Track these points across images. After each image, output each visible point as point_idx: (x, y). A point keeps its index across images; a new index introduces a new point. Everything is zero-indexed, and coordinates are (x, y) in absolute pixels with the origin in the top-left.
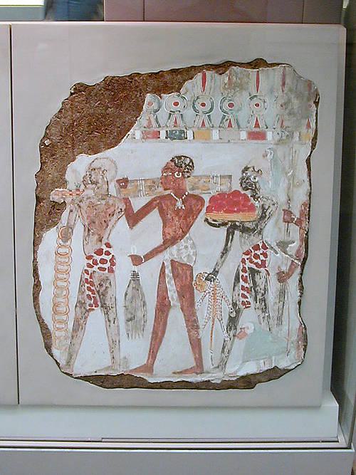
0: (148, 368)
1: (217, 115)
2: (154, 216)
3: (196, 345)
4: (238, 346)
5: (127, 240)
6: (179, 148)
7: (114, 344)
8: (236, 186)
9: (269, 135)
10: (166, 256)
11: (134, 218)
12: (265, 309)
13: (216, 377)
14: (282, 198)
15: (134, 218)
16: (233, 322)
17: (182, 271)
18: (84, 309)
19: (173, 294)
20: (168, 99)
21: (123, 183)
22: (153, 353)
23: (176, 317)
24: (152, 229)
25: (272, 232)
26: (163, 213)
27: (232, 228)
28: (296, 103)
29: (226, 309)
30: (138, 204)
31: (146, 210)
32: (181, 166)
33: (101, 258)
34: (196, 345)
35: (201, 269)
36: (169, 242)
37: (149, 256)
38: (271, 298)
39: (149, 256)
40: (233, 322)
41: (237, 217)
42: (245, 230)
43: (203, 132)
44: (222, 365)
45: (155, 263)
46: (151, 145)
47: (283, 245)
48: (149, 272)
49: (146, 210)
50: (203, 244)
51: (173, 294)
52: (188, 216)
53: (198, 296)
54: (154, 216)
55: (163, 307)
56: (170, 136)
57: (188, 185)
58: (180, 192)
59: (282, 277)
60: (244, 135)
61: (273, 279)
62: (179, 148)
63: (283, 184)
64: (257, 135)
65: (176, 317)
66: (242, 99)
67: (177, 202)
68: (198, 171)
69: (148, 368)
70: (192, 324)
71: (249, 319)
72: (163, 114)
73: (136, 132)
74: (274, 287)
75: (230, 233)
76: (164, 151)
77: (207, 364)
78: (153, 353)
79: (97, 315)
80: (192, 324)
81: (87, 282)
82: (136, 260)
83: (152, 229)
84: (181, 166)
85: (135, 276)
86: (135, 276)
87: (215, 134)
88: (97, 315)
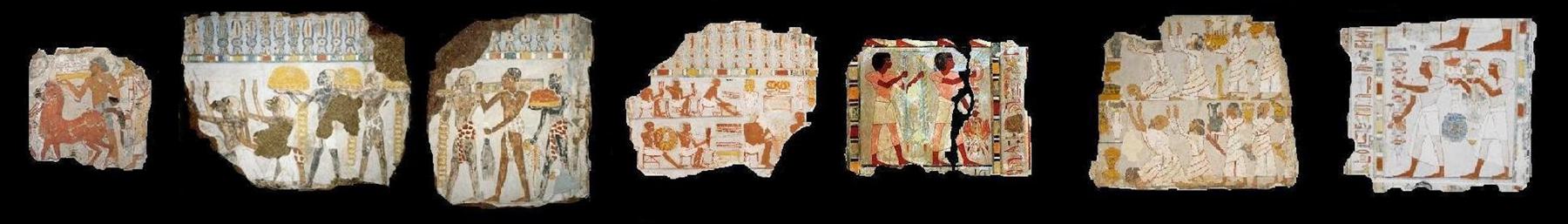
0: (496, 198)
1: (534, 46)
2: (498, 105)
3: (525, 184)
4: (552, 183)
5: (482, 119)
6: (511, 64)
7: (475, 184)
8: (546, 86)
9: (566, 55)
10: (506, 129)
11: (486, 107)
12: (566, 161)
13: (538, 203)
14: (574, 92)
15: (486, 107)
16: (547, 168)
17: (514, 137)
18: (456, 161)
19: (510, 152)
20: (505, 35)
21: (480, 85)
22: (498, 190)
23: (512, 166)
24: (497, 113)
25: (568, 113)
26: (503, 104)
27: (545, 110)
28: (581, 36)
29: (543, 161)
30: (488, 97)
31: (493, 101)
32: (513, 74)
33: (467, 127)
34: (525, 184)
35: (527, 136)
36: (507, 120)
37: (495, 129)
38: (570, 153)
39: (495, 129)
40: (547, 168)
41: (547, 105)
42: (552, 112)
43: (525, 54)
44: (541, 196)
45: (499, 133)
46: (495, 62)
47: (576, 121)
48: (495, 139)
49: (493, 101)
50: (528, 121)
51: (510, 152)
52: (519, 104)
53: (526, 152)
54: (498, 105)
55: (505, 160)
56: (507, 56)
57: (517, 85)
58: (513, 89)
59: (576, 141)
60: (550, 55)
61: (570, 141)
62: (511, 64)
63: (575, 84)
64: (558, 55)
65: (512, 166)
66: (549, 33)
67: (511, 94)
68: (523, 76)
69: (496, 198)
70: (522, 170)
71: (557, 167)
72: (502, 44)
73: (487, 55)
74: (571, 146)
75: (543, 115)
76: (503, 65)
77: (532, 196)
78: (498, 190)
79: (464, 166)
80: (522, 170)
81: (458, 145)
82: (487, 131)
83: (497, 113)
84: (513, 74)
85: (487, 141)
86: (487, 141)
87: (533, 55)
88: (464, 166)
